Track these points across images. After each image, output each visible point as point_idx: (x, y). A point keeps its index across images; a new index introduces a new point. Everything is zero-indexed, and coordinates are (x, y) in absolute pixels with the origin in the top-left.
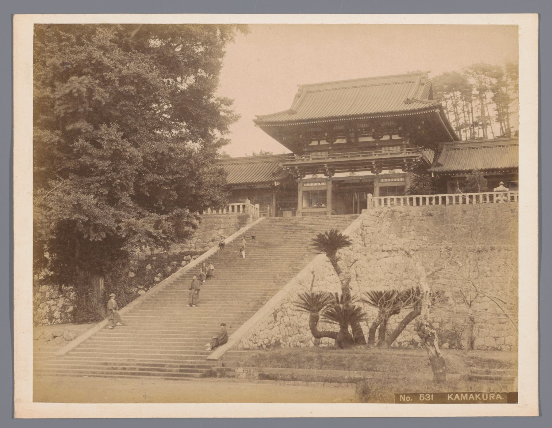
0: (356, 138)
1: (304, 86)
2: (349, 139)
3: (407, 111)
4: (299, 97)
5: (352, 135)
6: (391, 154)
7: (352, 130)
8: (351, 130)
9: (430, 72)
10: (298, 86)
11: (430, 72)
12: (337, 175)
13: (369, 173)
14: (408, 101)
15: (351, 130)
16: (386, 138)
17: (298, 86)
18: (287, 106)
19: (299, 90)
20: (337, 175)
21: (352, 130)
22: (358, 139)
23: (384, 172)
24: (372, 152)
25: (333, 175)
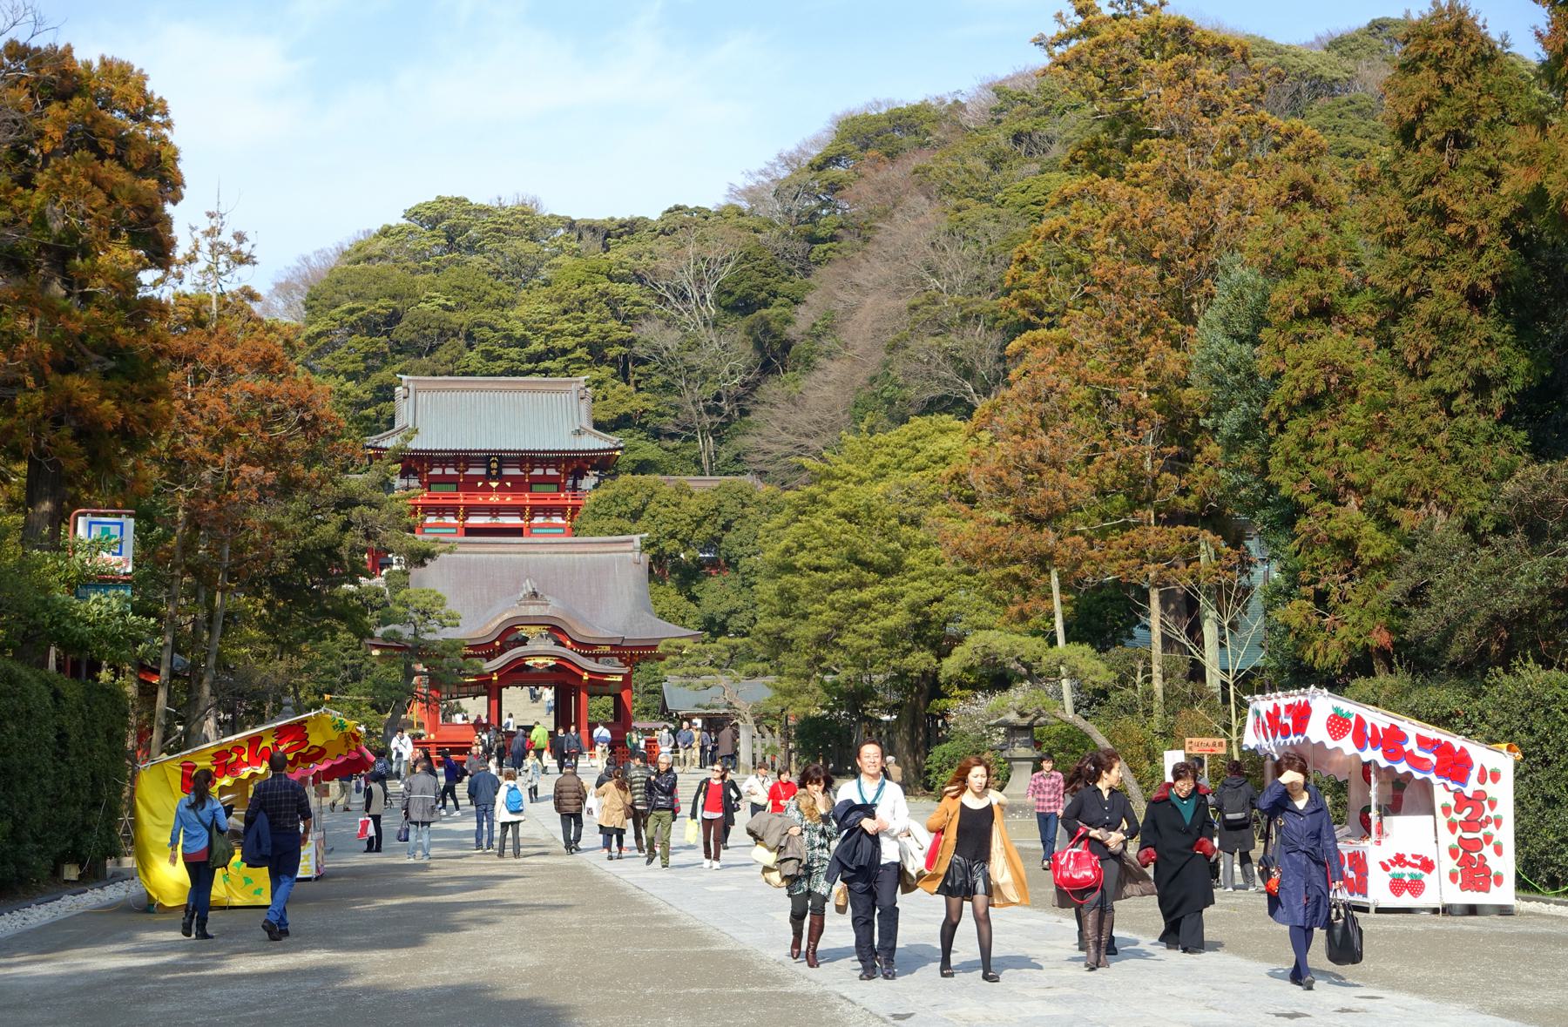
0: (499, 470)
2: (489, 469)
5: (494, 465)
16: (538, 472)
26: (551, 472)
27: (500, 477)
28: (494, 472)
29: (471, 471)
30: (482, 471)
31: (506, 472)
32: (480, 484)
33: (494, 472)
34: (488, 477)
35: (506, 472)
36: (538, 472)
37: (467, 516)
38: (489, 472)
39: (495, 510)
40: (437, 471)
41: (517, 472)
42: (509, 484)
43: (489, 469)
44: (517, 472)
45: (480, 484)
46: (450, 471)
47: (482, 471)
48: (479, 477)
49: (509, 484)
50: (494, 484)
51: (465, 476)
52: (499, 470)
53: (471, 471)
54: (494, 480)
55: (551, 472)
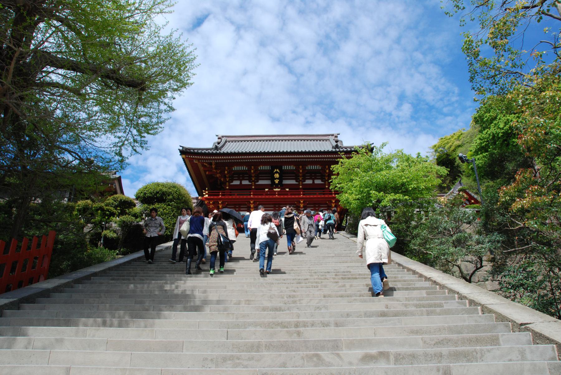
5: (277, 176)
16: (309, 182)
22: (282, 181)
26: (318, 182)
28: (277, 181)
29: (261, 182)
30: (268, 182)
33: (277, 181)
34: (273, 185)
35: (286, 182)
36: (309, 182)
41: (293, 182)
43: (273, 179)
44: (293, 182)
47: (268, 182)
49: (287, 190)
51: (255, 185)
52: (281, 179)
53: (261, 182)
55: (318, 182)
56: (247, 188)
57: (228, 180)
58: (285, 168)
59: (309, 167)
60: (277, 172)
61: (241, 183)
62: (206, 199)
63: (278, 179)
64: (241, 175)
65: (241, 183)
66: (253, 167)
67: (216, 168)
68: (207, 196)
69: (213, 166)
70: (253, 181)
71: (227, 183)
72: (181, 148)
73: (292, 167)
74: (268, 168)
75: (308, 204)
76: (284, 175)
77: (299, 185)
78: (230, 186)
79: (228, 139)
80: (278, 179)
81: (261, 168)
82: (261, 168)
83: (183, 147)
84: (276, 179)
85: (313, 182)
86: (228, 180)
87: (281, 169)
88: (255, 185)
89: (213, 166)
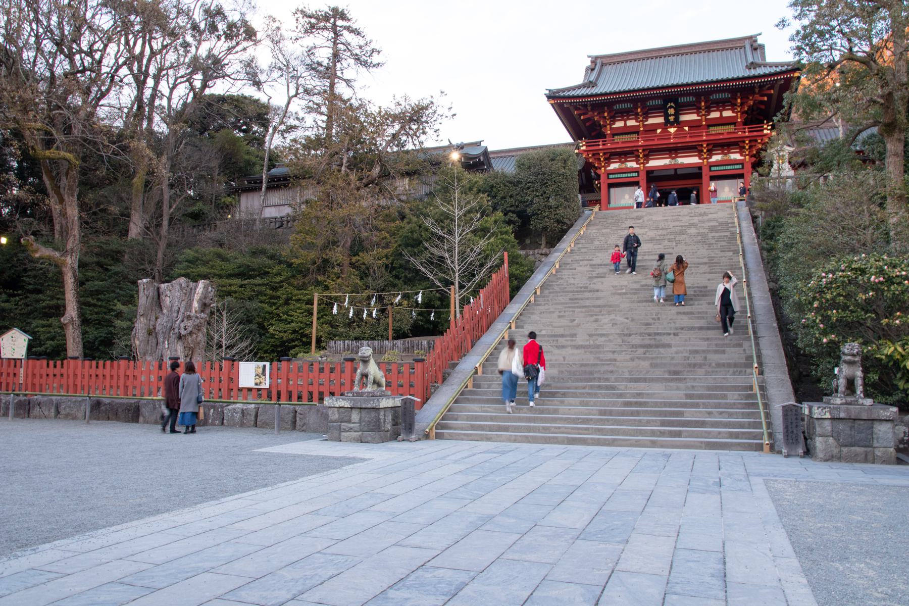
0: (677, 115)
1: (597, 58)
2: (666, 116)
3: (749, 78)
4: (593, 70)
5: (671, 111)
6: (728, 133)
7: (672, 104)
8: (669, 105)
9: (760, 34)
10: (589, 57)
11: (760, 34)
12: (653, 163)
13: (694, 160)
14: (753, 65)
15: (669, 105)
17: (589, 57)
18: (579, 80)
19: (592, 62)
20: (653, 163)
21: (672, 104)
23: (716, 158)
24: (702, 132)
25: (648, 163)
26: (728, 114)
27: (677, 123)
28: (672, 118)
29: (651, 121)
30: (661, 120)
31: (684, 118)
32: (659, 131)
33: (672, 118)
37: (647, 158)
38: (667, 119)
39: (673, 150)
40: (619, 124)
41: (694, 117)
42: (686, 128)
44: (694, 117)
45: (659, 131)
46: (631, 123)
47: (661, 120)
48: (658, 126)
50: (672, 130)
52: (677, 115)
53: (651, 121)
54: (672, 125)
56: (634, 131)
57: (608, 122)
58: (682, 100)
59: (715, 97)
60: (671, 107)
61: (625, 124)
62: (584, 151)
63: (673, 115)
64: (625, 114)
65: (625, 124)
66: (639, 104)
67: (592, 110)
68: (584, 148)
69: (589, 108)
70: (641, 121)
71: (608, 126)
72: (547, 92)
73: (691, 99)
74: (659, 102)
75: (713, 147)
76: (681, 108)
77: (700, 121)
78: (611, 129)
79: (605, 61)
80: (673, 115)
81: (651, 103)
82: (651, 103)
83: (550, 90)
84: (671, 115)
85: (721, 114)
86: (608, 122)
87: (676, 102)
88: (644, 126)
89: (589, 108)
